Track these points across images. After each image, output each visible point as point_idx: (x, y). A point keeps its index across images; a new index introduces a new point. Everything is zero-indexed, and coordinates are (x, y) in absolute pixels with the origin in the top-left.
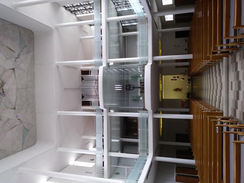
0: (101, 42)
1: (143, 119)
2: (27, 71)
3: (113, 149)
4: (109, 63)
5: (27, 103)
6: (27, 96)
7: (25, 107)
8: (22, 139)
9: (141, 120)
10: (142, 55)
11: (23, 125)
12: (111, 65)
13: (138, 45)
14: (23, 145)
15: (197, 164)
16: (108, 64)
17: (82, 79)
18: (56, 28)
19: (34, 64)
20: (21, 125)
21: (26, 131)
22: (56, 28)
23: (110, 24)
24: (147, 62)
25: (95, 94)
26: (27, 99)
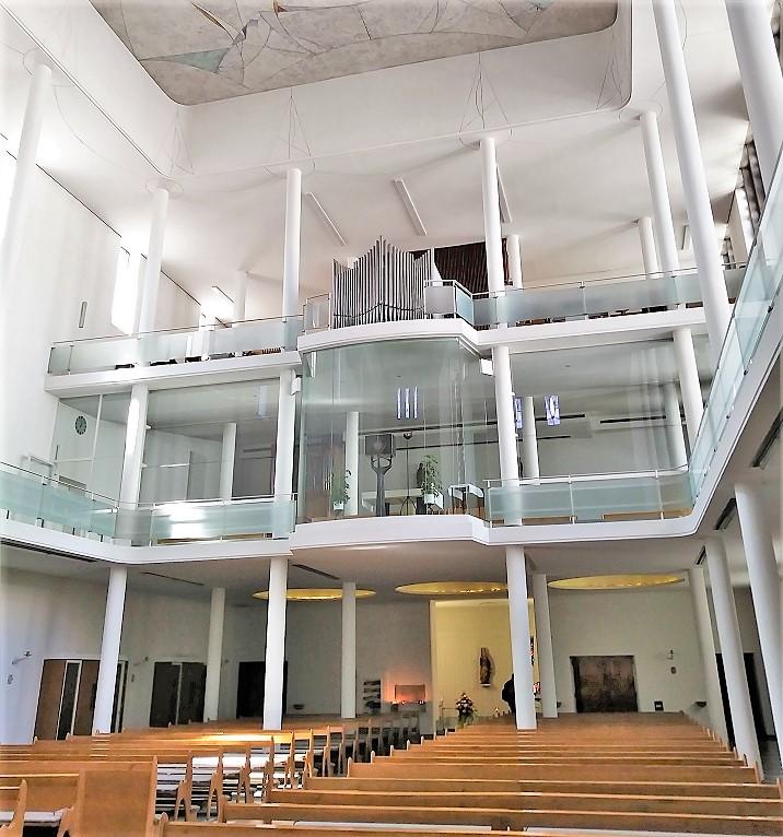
0: (579, 316)
1: (266, 517)
2: (438, 28)
3: (158, 397)
4: (489, 357)
5: (314, 48)
6: (344, 45)
7: (300, 45)
8: (179, 52)
9: (265, 508)
10: (531, 498)
11: (228, 49)
12: (480, 368)
13: (570, 480)
14: (156, 59)
15: (95, 738)
16: (487, 354)
17: (417, 255)
18: (638, 118)
19: (480, 49)
20: (228, 44)
21: (216, 61)
22: (638, 118)
23: (666, 348)
24: (499, 522)
25: (357, 312)
26: (332, 48)
